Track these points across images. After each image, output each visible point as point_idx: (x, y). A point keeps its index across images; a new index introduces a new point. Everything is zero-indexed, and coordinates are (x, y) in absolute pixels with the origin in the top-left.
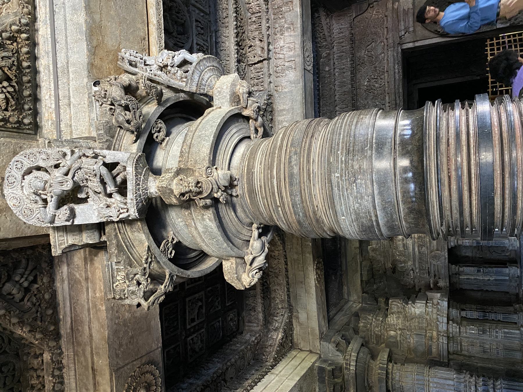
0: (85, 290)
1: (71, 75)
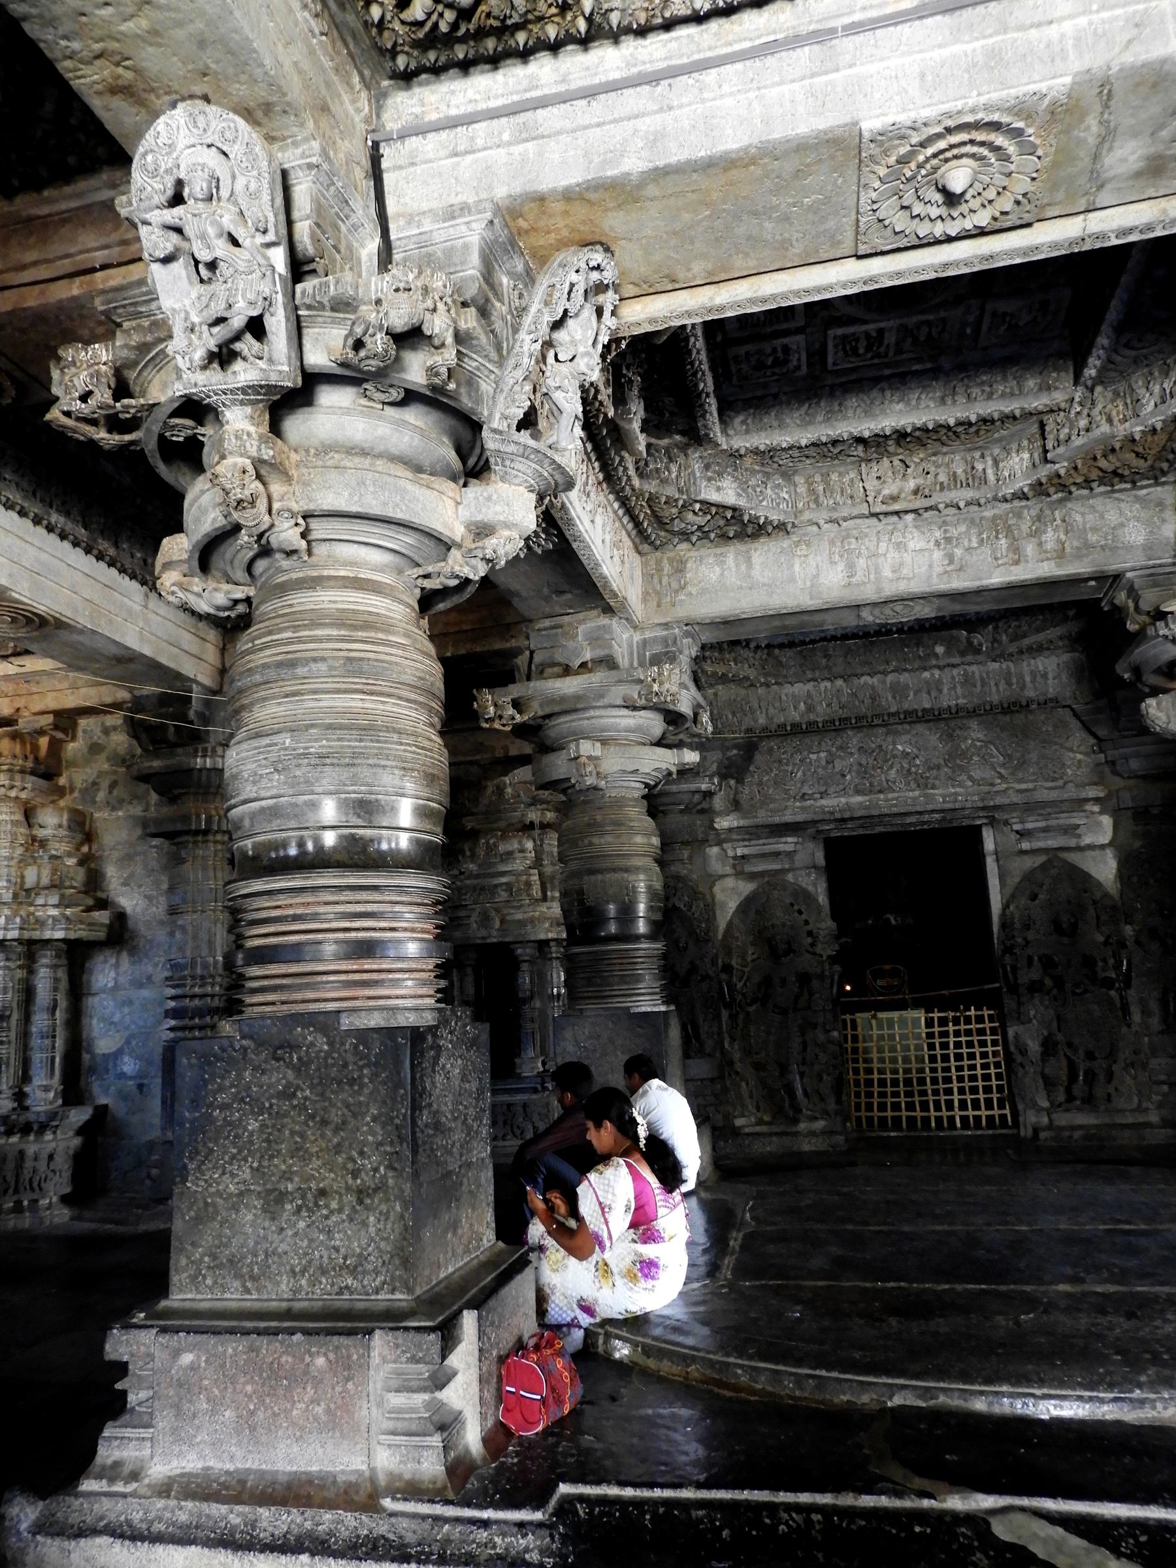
0: (104, 241)
1: (517, 149)
